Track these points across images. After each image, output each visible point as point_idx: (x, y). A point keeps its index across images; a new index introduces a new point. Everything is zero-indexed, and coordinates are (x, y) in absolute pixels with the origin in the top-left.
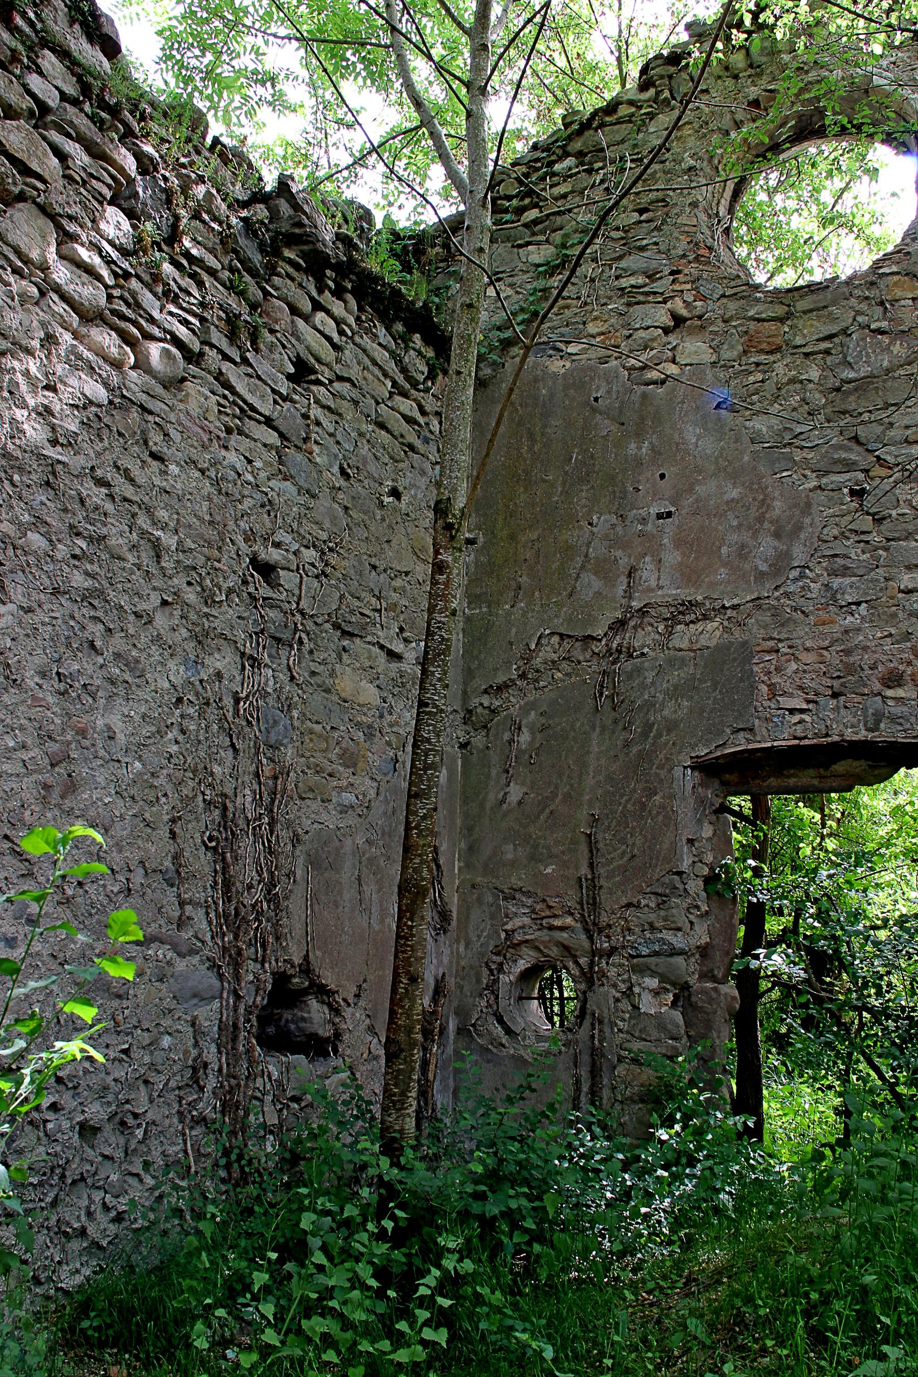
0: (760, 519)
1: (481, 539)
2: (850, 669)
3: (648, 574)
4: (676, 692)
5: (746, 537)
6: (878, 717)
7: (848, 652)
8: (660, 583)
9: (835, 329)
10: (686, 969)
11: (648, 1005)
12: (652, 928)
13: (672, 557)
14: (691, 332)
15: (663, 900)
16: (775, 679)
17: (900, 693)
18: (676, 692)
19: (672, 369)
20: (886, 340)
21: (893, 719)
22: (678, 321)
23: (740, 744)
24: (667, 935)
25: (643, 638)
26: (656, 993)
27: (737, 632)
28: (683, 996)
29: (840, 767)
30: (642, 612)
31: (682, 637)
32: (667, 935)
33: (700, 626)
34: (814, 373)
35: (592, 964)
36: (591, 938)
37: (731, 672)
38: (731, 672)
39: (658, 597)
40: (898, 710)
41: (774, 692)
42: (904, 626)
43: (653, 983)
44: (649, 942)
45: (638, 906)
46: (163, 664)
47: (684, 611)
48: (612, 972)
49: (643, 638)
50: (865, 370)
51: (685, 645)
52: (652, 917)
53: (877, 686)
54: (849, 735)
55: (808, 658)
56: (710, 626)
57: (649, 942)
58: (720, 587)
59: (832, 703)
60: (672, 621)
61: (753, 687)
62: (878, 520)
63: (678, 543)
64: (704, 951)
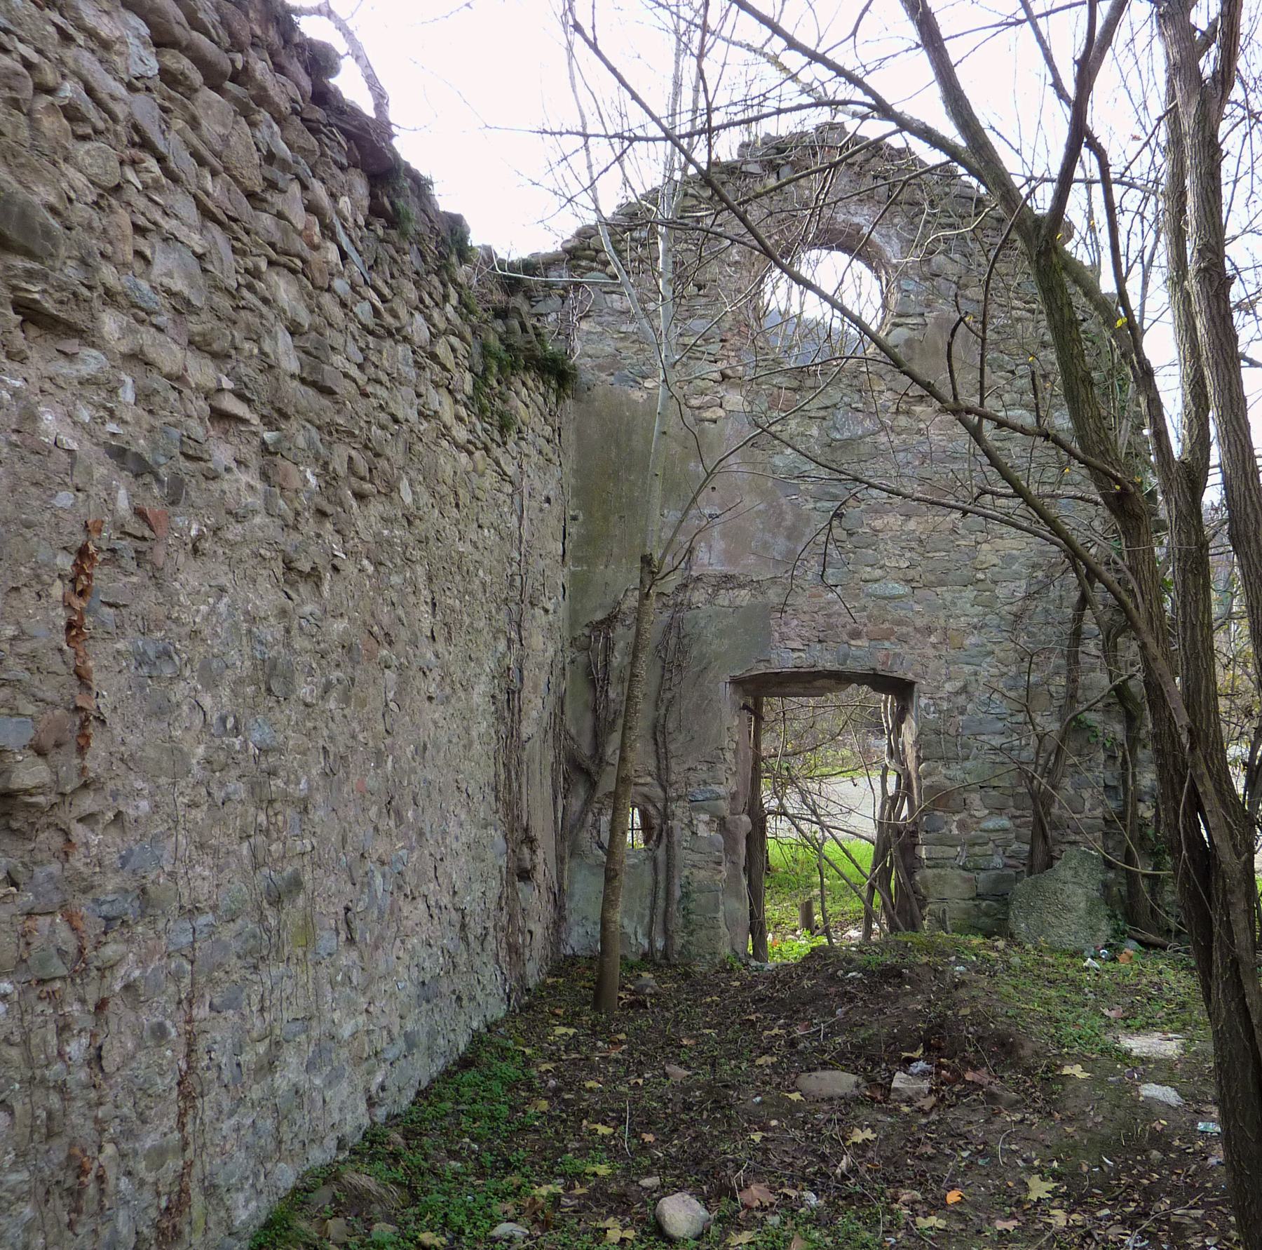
0: (779, 525)
1: (581, 518)
2: (831, 627)
3: (702, 555)
4: (721, 634)
5: (768, 537)
6: (846, 656)
7: (829, 616)
8: (709, 560)
9: (829, 403)
10: (724, 807)
11: (702, 831)
12: (705, 783)
13: (719, 545)
14: (734, 386)
15: (711, 764)
16: (784, 629)
17: (859, 643)
18: (721, 634)
19: (721, 413)
20: (860, 415)
21: (855, 658)
22: (724, 377)
23: (762, 669)
24: (715, 787)
25: (698, 596)
26: (707, 824)
27: (760, 598)
28: (722, 825)
29: (818, 683)
30: (698, 579)
31: (724, 598)
32: (715, 787)
33: (736, 592)
34: (815, 431)
35: (665, 808)
36: (665, 791)
37: (758, 622)
38: (758, 622)
39: (709, 570)
40: (859, 653)
41: (783, 638)
42: (863, 602)
43: (706, 817)
44: (702, 792)
45: (695, 770)
46: (233, 545)
47: (727, 581)
48: (679, 812)
49: (698, 596)
50: (847, 434)
51: (726, 603)
52: (704, 776)
53: (845, 638)
54: (828, 666)
55: (807, 617)
56: (743, 592)
57: (702, 792)
58: (749, 566)
59: (818, 646)
60: (717, 588)
61: (770, 634)
62: (850, 535)
63: (724, 535)
64: (734, 797)
